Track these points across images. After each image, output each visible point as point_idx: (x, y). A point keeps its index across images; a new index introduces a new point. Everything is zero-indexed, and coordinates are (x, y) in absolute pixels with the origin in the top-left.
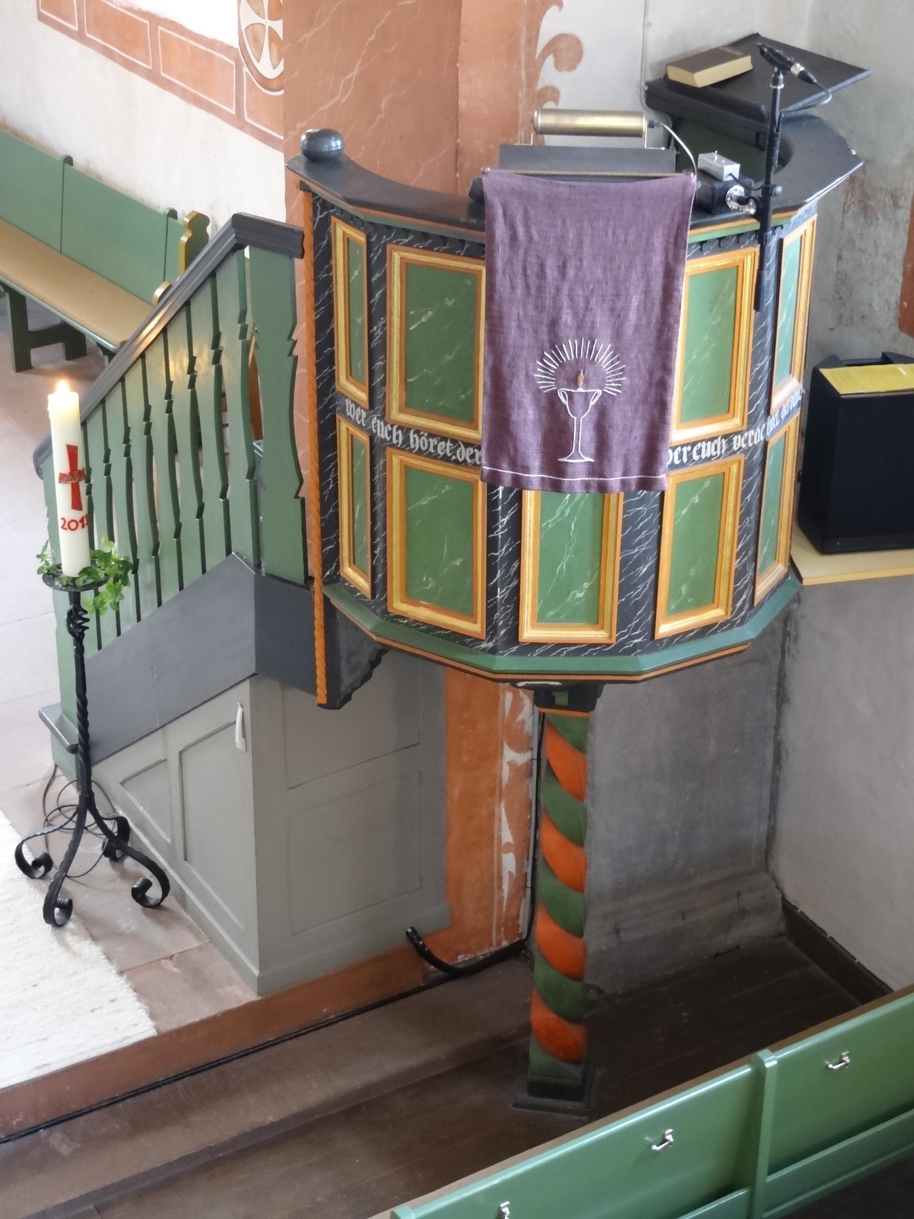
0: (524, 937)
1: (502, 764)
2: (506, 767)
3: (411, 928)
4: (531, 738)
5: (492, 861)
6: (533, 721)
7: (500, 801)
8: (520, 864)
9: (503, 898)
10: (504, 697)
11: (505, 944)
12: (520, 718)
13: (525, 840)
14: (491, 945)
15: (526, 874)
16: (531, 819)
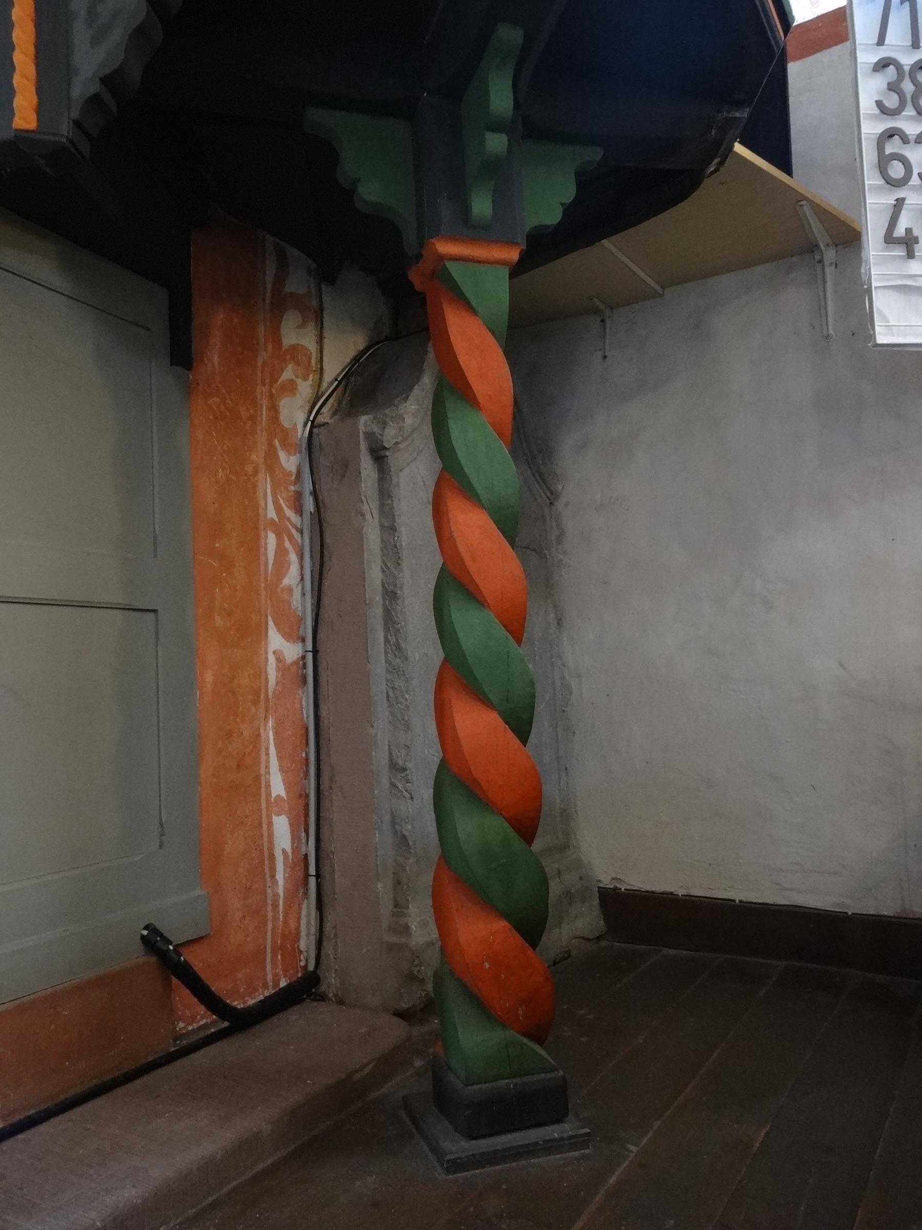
0: (311, 968)
1: (266, 653)
2: (272, 660)
3: (146, 928)
4: (301, 620)
5: (260, 824)
6: (303, 588)
7: (266, 718)
8: (295, 838)
9: (278, 895)
10: (266, 537)
11: (283, 983)
12: (286, 581)
13: (300, 796)
14: (265, 986)
15: (306, 855)
16: (307, 759)
